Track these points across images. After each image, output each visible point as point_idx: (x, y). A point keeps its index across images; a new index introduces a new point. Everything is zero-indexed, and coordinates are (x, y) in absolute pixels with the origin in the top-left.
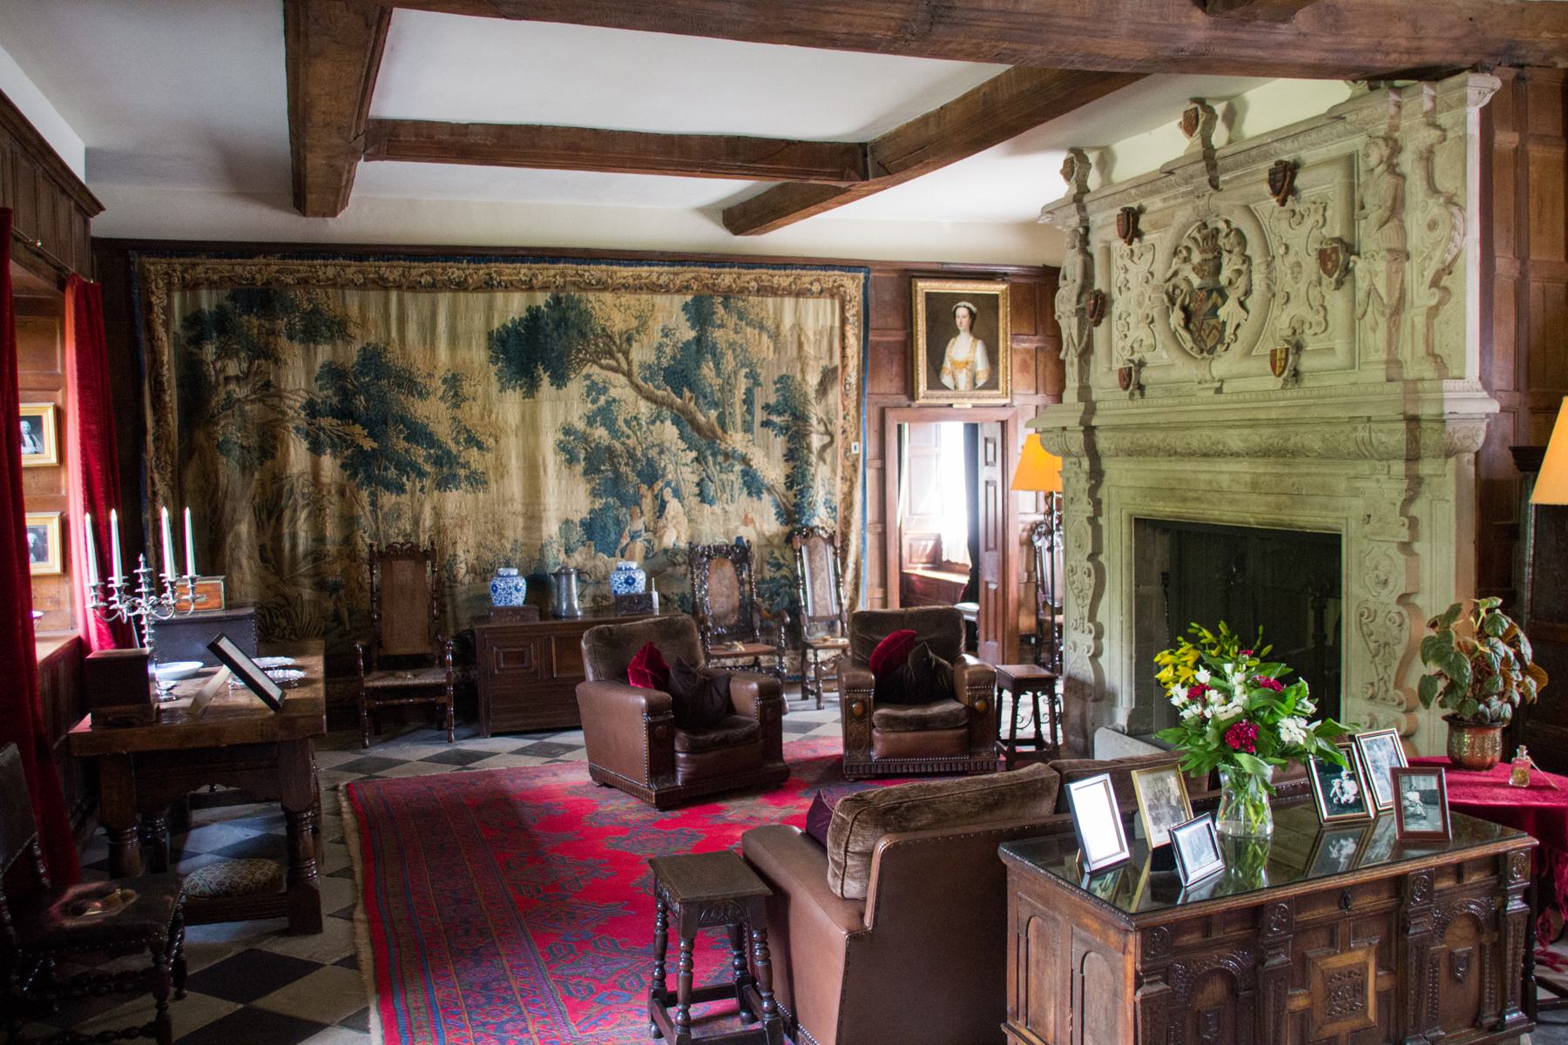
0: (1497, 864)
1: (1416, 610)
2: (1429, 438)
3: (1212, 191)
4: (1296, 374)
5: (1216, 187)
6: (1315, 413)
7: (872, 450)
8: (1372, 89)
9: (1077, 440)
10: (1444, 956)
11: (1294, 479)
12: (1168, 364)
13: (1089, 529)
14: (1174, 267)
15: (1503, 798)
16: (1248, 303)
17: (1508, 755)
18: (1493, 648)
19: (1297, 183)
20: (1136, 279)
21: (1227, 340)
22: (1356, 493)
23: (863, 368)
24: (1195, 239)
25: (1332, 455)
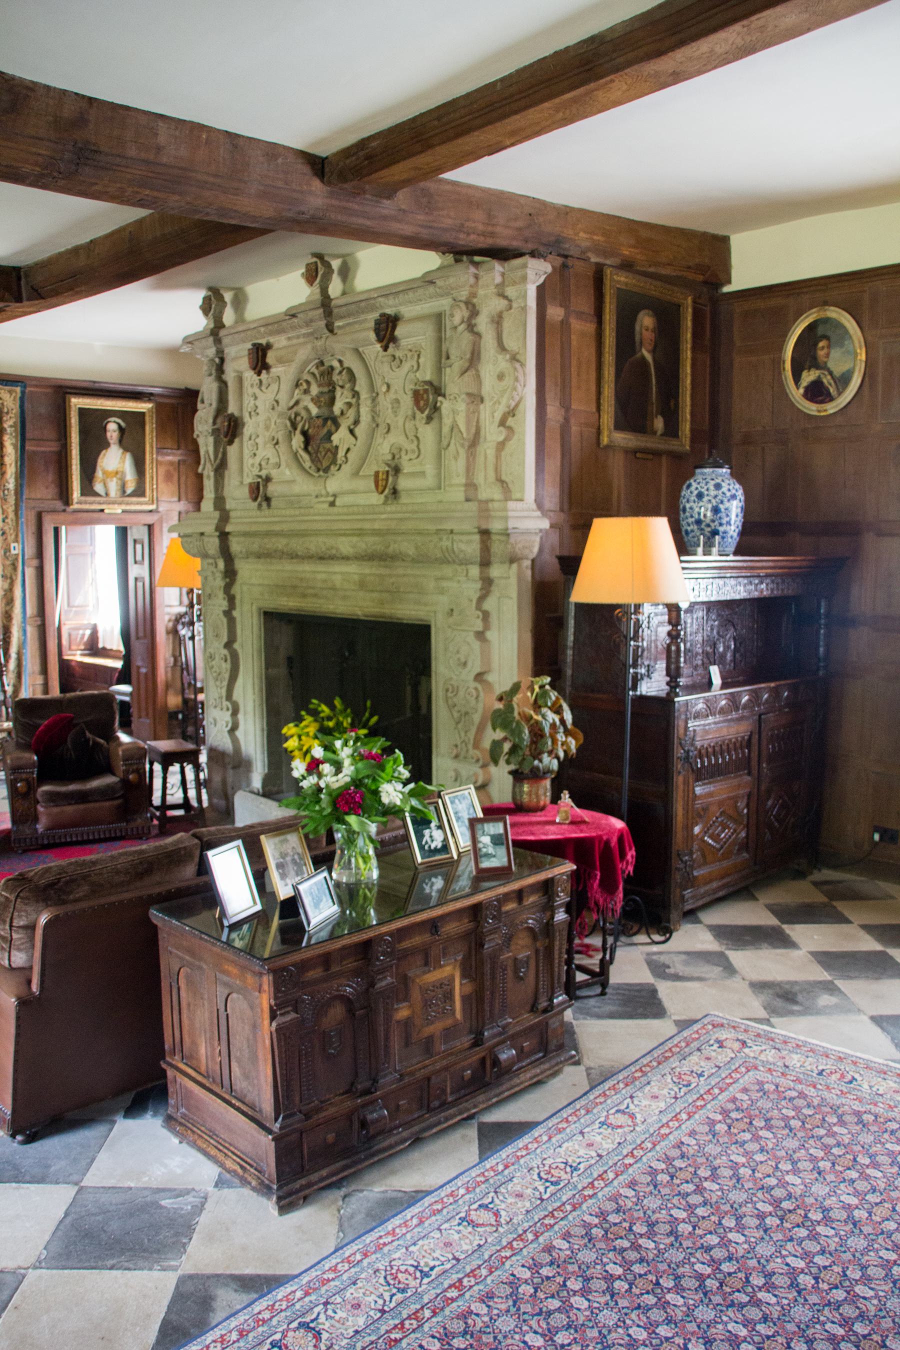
0: (547, 887)
1: (488, 686)
2: (497, 548)
3: (328, 334)
4: (395, 492)
5: (331, 331)
6: (409, 525)
7: (30, 551)
8: (457, 261)
9: (213, 544)
10: (510, 963)
11: (393, 580)
12: (291, 479)
13: (225, 620)
14: (296, 398)
15: (552, 834)
16: (357, 431)
17: (556, 799)
18: (544, 716)
19: (397, 332)
20: (264, 404)
21: (339, 462)
22: (442, 591)
23: (20, 475)
24: (313, 374)
25: (422, 559)
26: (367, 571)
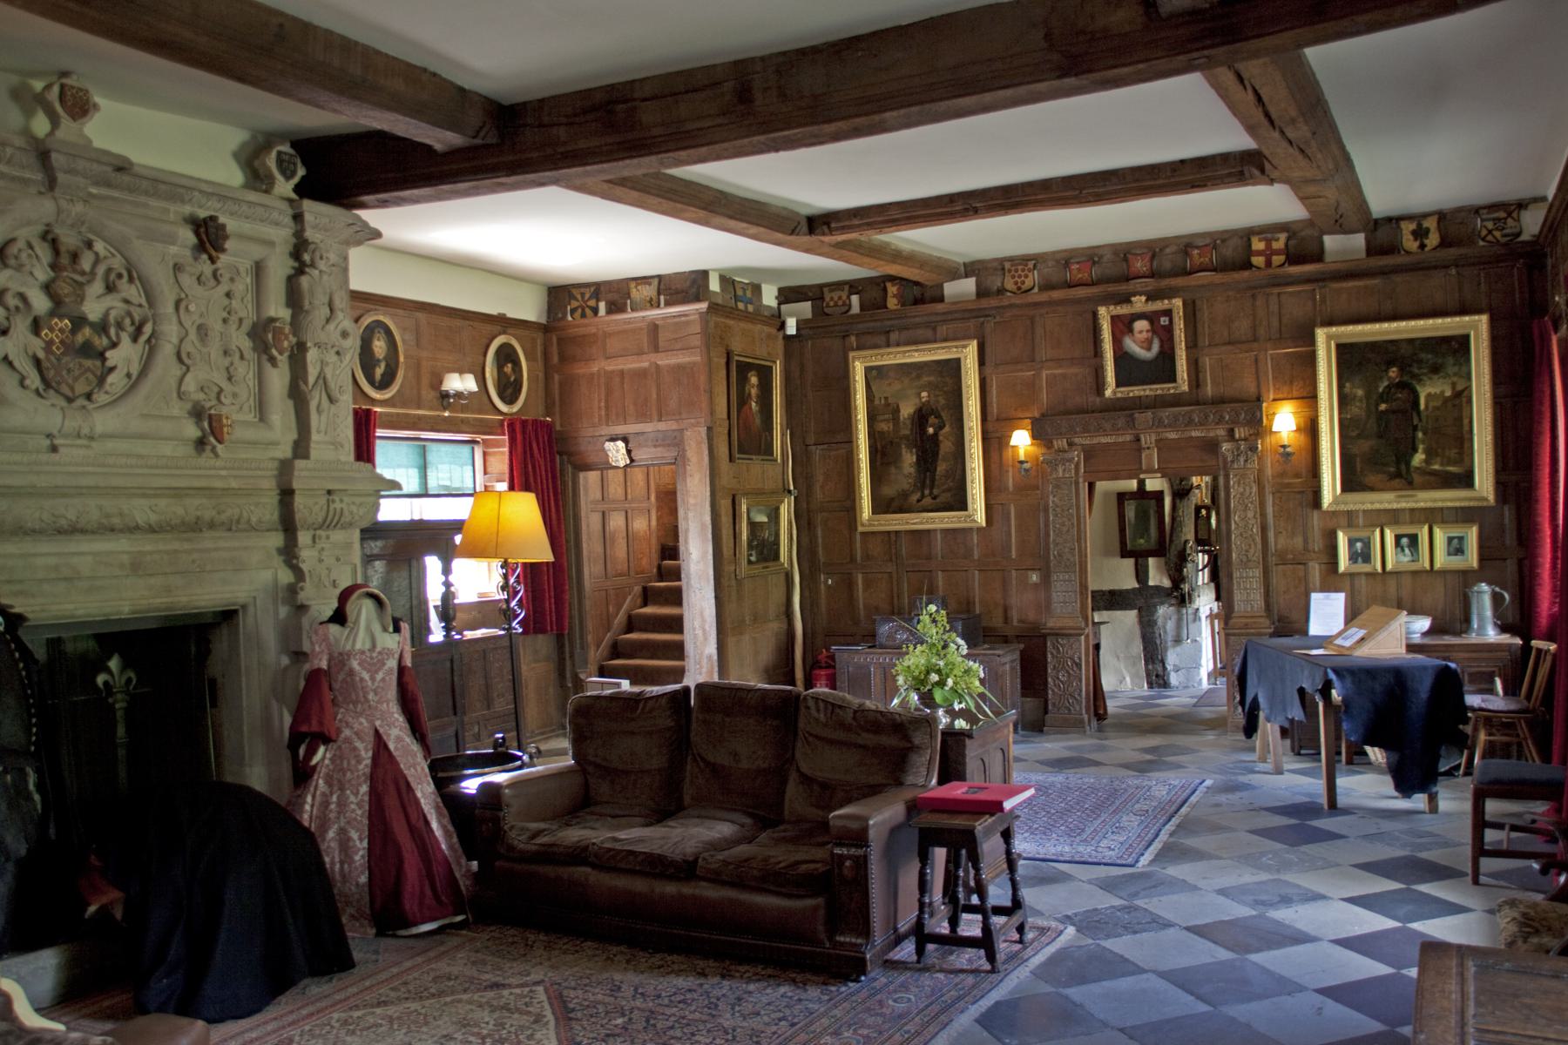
26: (148, 548)
